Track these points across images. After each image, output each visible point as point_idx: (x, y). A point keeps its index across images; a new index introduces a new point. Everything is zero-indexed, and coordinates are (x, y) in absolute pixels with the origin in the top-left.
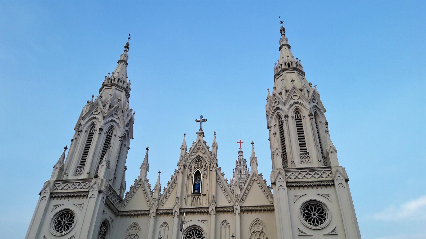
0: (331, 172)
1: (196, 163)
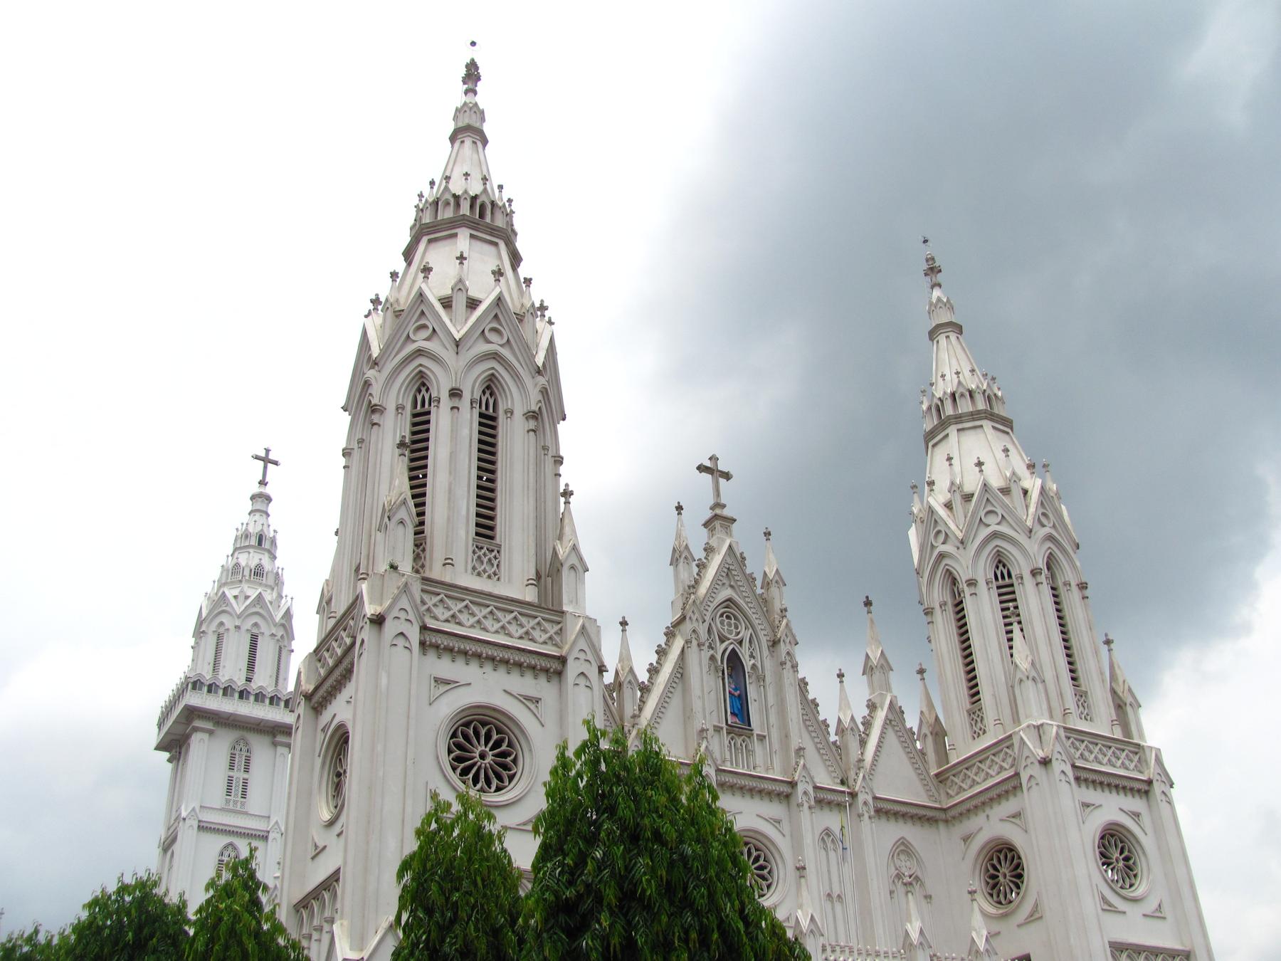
0: (561, 629)
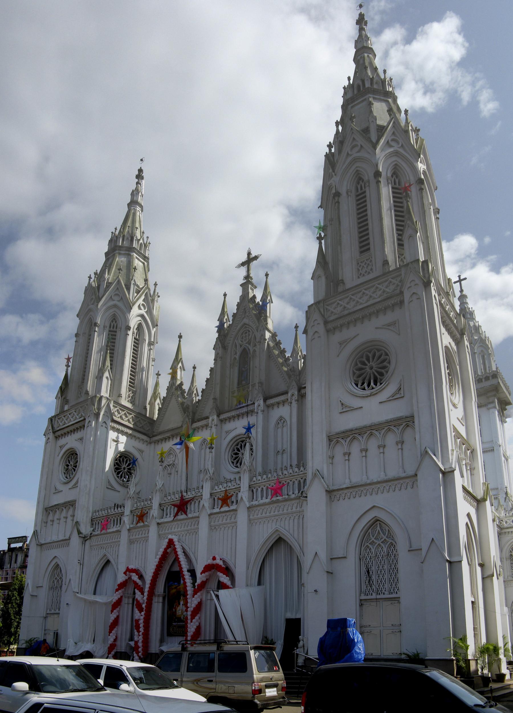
1: (242, 338)
